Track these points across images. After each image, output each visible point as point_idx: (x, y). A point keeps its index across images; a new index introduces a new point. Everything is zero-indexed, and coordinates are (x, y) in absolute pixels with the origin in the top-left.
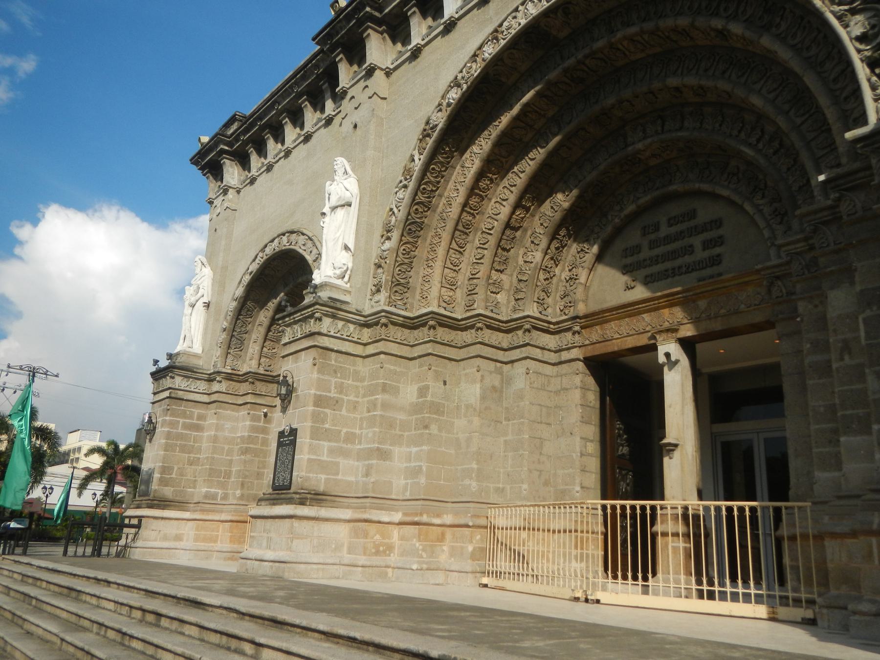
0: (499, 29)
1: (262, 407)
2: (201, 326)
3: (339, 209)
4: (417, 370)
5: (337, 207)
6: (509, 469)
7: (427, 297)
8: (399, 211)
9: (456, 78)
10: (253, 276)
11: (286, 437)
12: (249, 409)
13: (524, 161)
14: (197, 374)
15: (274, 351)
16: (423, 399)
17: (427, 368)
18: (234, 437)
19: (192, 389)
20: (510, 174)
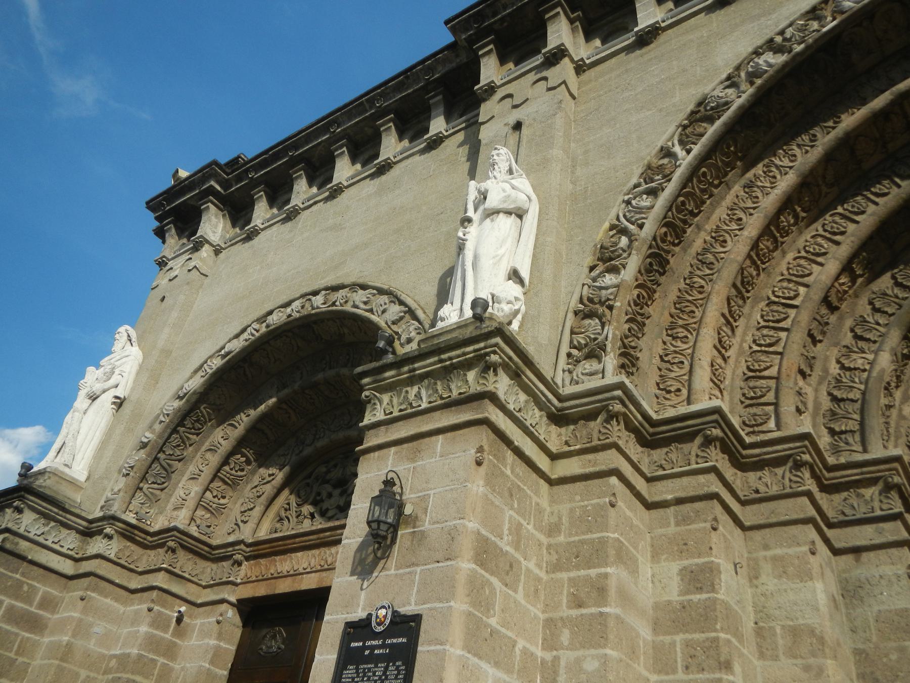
1: (178, 601)
2: (98, 434)
4: (672, 529)
5: (497, 212)
7: (679, 390)
9: (771, 40)
10: (228, 362)
11: (376, 636)
12: (153, 601)
13: (859, 198)
14: (68, 516)
15: (222, 501)
16: (704, 596)
17: (708, 525)
18: (104, 656)
19: (49, 543)
20: (827, 217)
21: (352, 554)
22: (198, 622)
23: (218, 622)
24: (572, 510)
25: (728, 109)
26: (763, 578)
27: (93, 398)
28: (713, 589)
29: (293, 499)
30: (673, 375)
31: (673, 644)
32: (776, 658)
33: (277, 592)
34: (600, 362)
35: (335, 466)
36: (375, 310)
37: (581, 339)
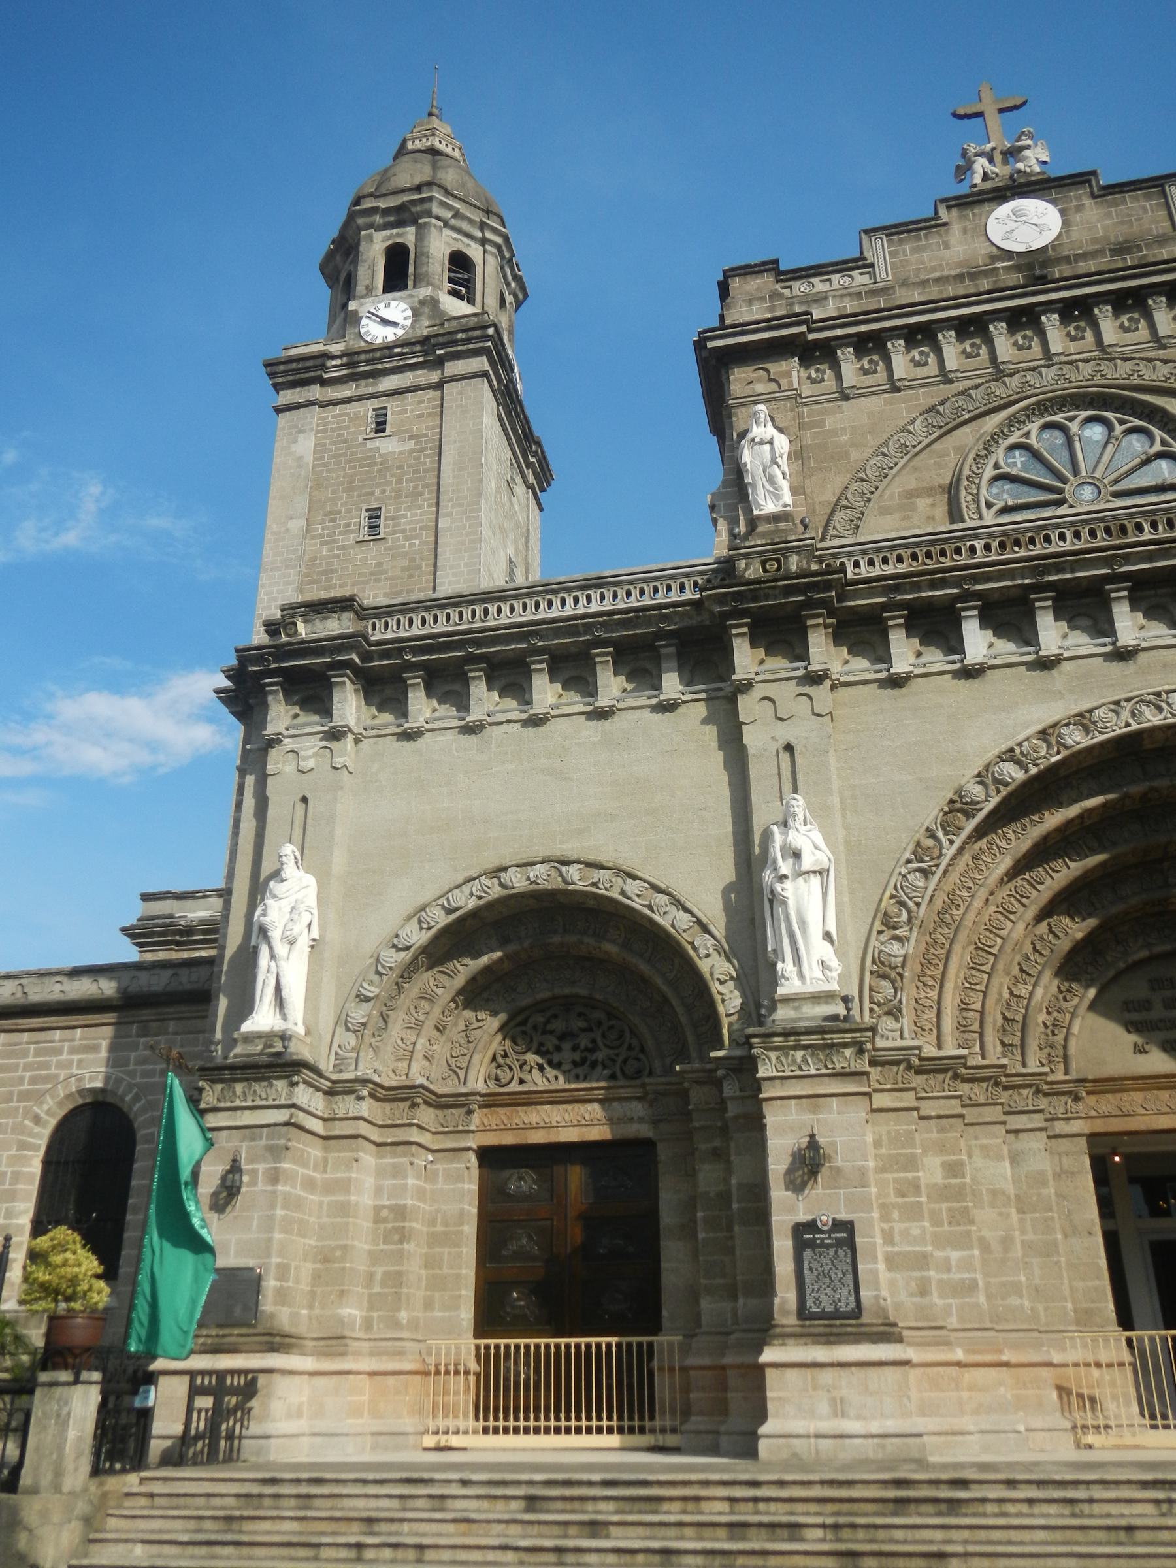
0: (1088, 715)
3: (812, 875)
4: (935, 1135)
6: (1037, 1281)
8: (918, 904)
9: (1012, 750)
11: (822, 1232)
12: (413, 1155)
13: (1041, 869)
14: (323, 1081)
20: (1018, 879)
21: (782, 1176)
22: (439, 1166)
23: (468, 1168)
24: (889, 1132)
25: (981, 809)
26: (975, 1158)
27: (292, 943)
28: (963, 1176)
29: (508, 1043)
30: (926, 1017)
31: (940, 1209)
32: (983, 1208)
33: (530, 1141)
34: (897, 1020)
35: (555, 1016)
36: (655, 909)
37: (879, 997)
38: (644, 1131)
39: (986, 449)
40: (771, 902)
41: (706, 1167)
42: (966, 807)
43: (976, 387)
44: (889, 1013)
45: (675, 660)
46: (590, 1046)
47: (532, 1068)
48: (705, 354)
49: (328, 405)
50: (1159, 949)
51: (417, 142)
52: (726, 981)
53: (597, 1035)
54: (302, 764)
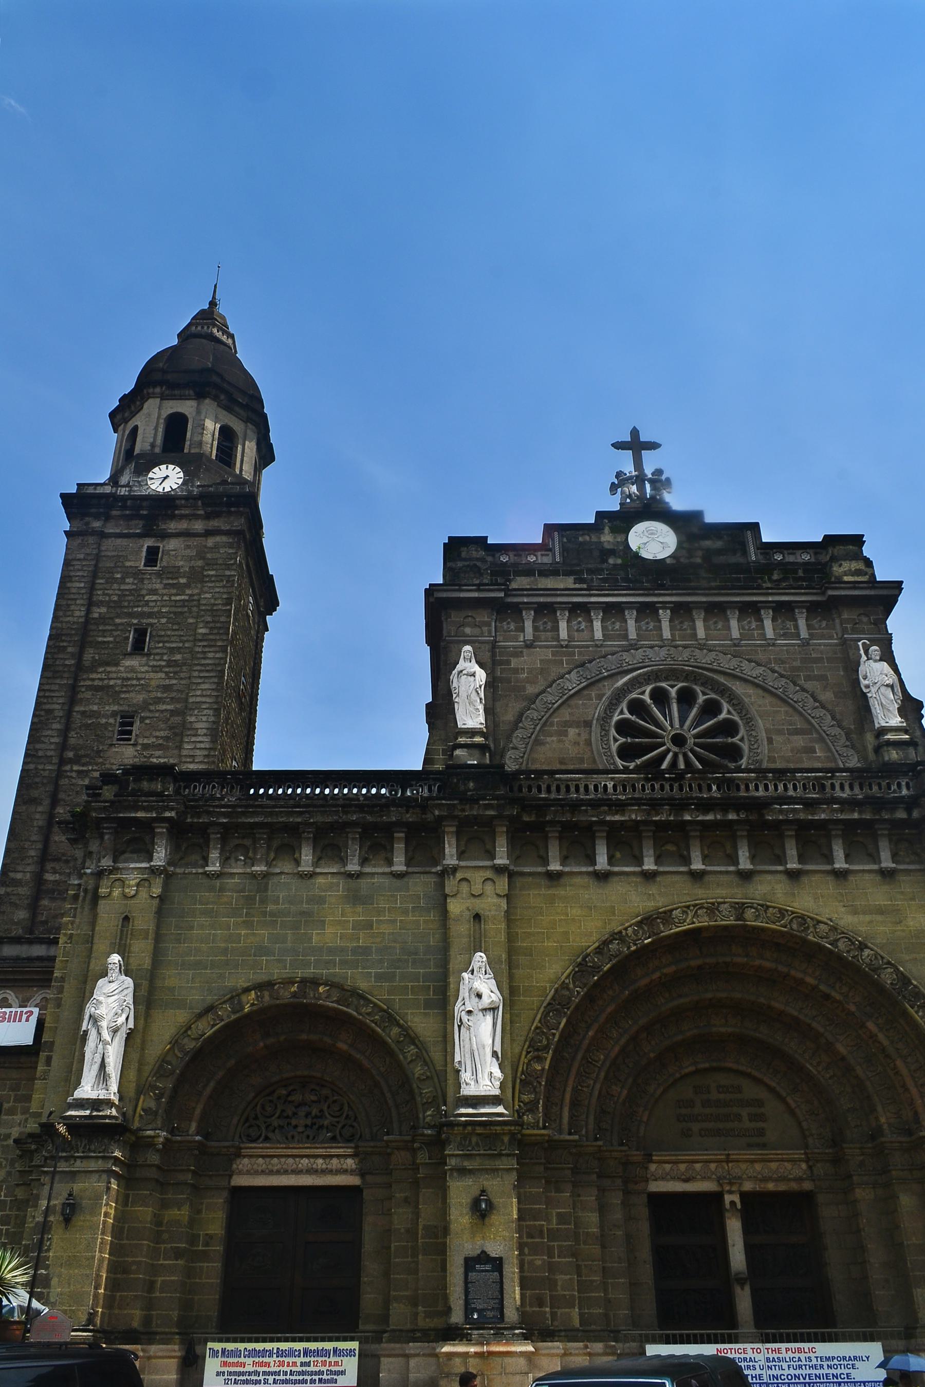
4: (553, 1194)
7: (555, 1120)
9: (620, 932)
25: (599, 972)
27: (115, 1031)
37: (525, 1098)
38: (354, 1180)
39: (616, 699)
40: (459, 1027)
41: (401, 1210)
42: (590, 969)
43: (613, 654)
44: (531, 1111)
45: (404, 842)
46: (318, 1114)
47: (275, 1128)
48: (432, 600)
49: (111, 537)
50: (702, 1066)
51: (199, 328)
52: (424, 1079)
53: (325, 1108)
54: (127, 890)
